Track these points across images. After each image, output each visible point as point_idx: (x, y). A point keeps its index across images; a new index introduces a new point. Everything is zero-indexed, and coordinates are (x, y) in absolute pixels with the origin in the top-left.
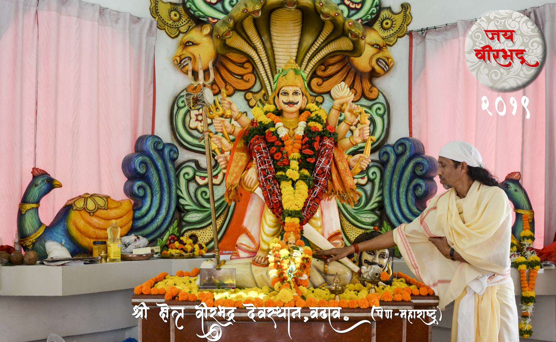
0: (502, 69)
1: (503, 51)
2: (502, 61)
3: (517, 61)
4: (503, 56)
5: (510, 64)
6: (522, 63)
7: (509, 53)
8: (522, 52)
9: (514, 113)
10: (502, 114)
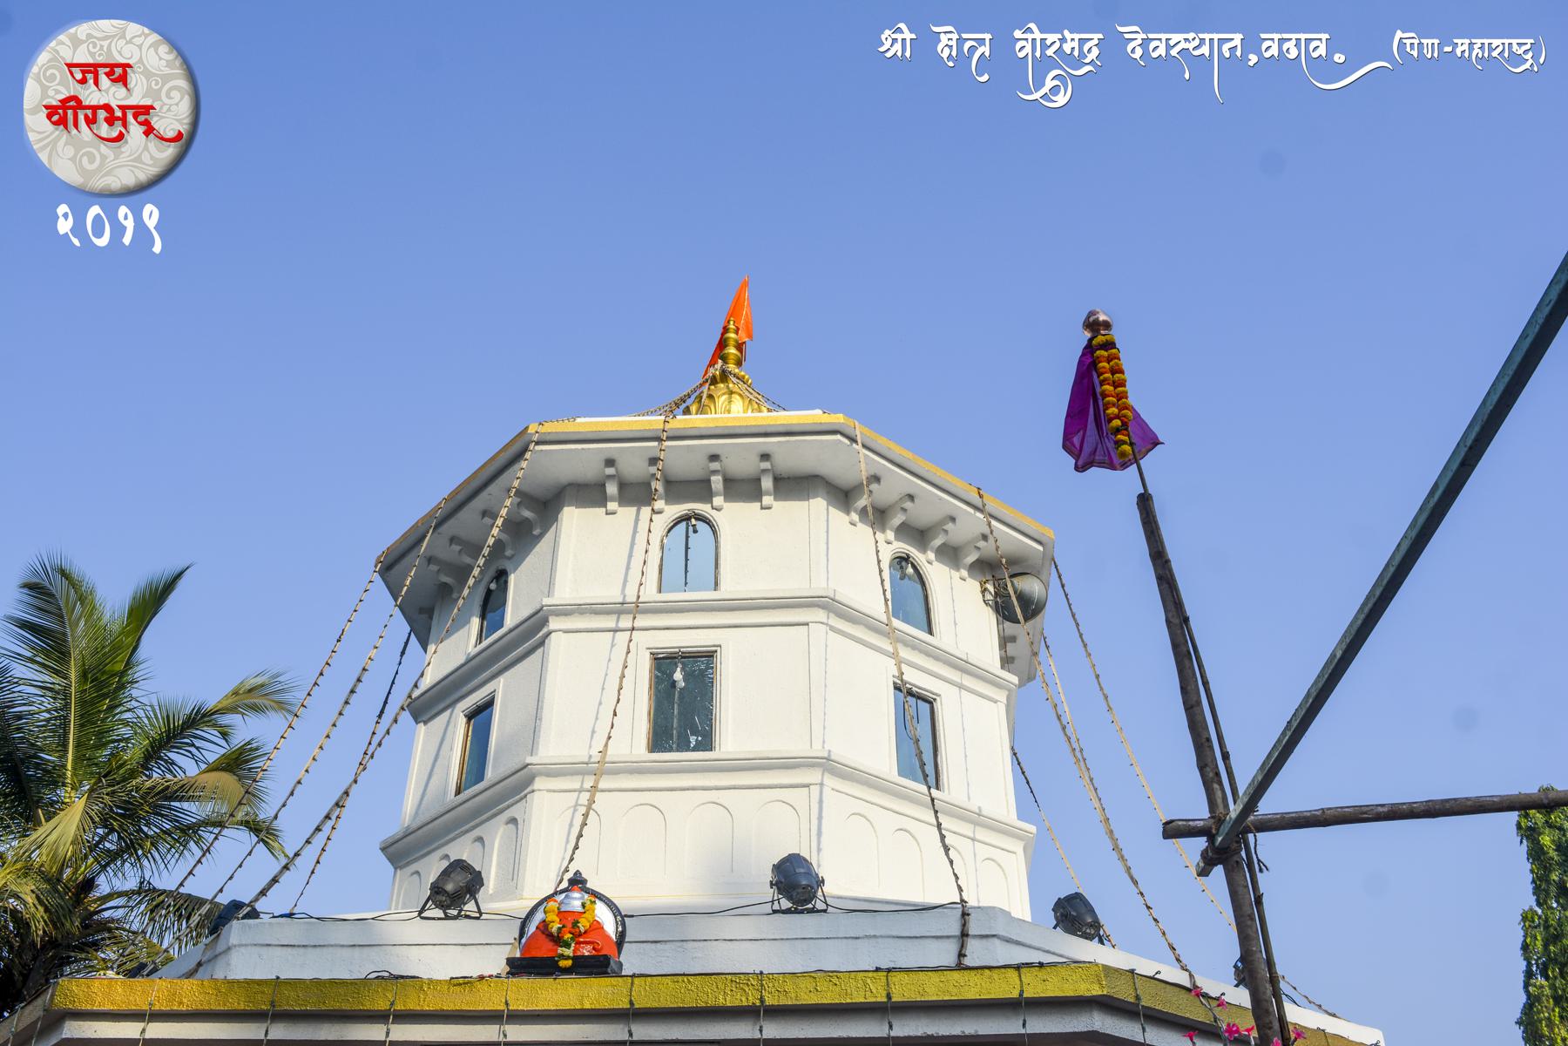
0: (105, 148)
1: (107, 107)
2: (104, 130)
3: (135, 130)
4: (106, 120)
5: (120, 137)
6: (147, 133)
7: (118, 113)
8: (147, 109)
9: (127, 240)
10: (102, 242)
